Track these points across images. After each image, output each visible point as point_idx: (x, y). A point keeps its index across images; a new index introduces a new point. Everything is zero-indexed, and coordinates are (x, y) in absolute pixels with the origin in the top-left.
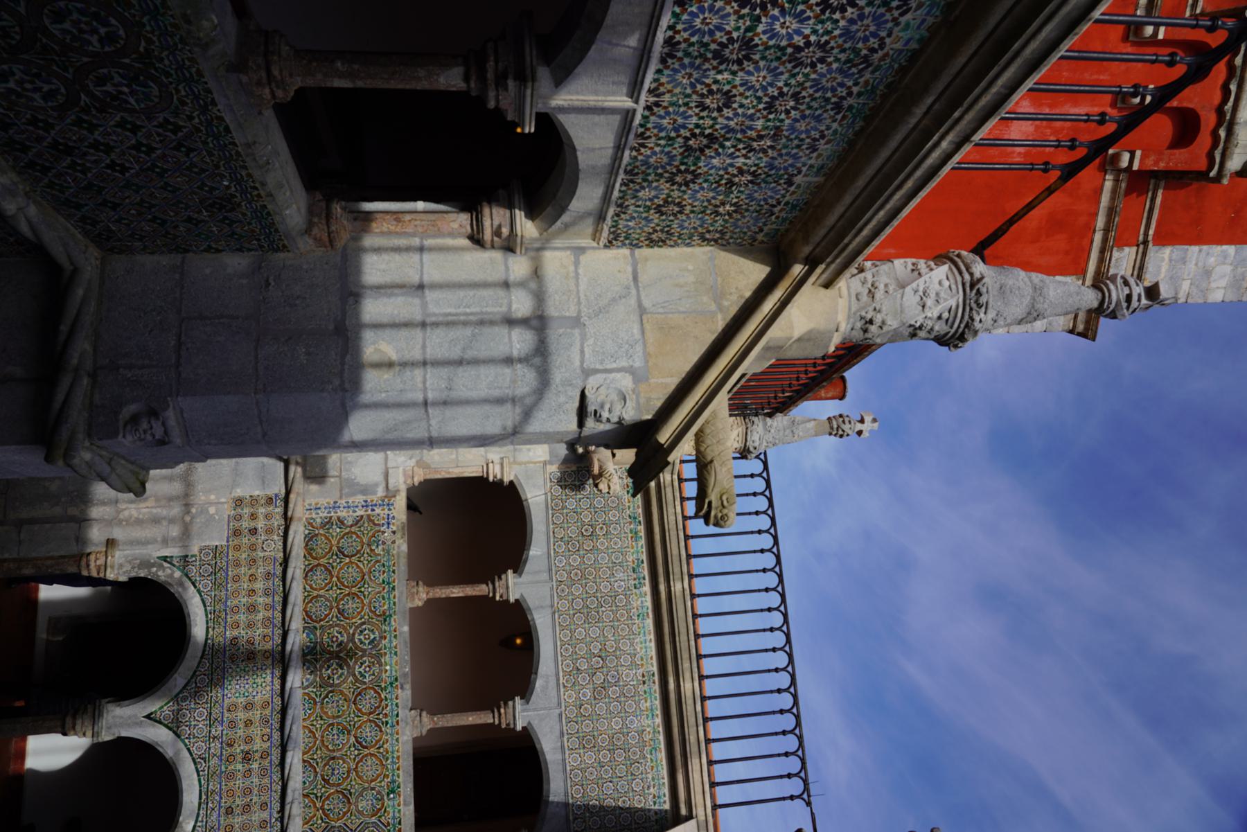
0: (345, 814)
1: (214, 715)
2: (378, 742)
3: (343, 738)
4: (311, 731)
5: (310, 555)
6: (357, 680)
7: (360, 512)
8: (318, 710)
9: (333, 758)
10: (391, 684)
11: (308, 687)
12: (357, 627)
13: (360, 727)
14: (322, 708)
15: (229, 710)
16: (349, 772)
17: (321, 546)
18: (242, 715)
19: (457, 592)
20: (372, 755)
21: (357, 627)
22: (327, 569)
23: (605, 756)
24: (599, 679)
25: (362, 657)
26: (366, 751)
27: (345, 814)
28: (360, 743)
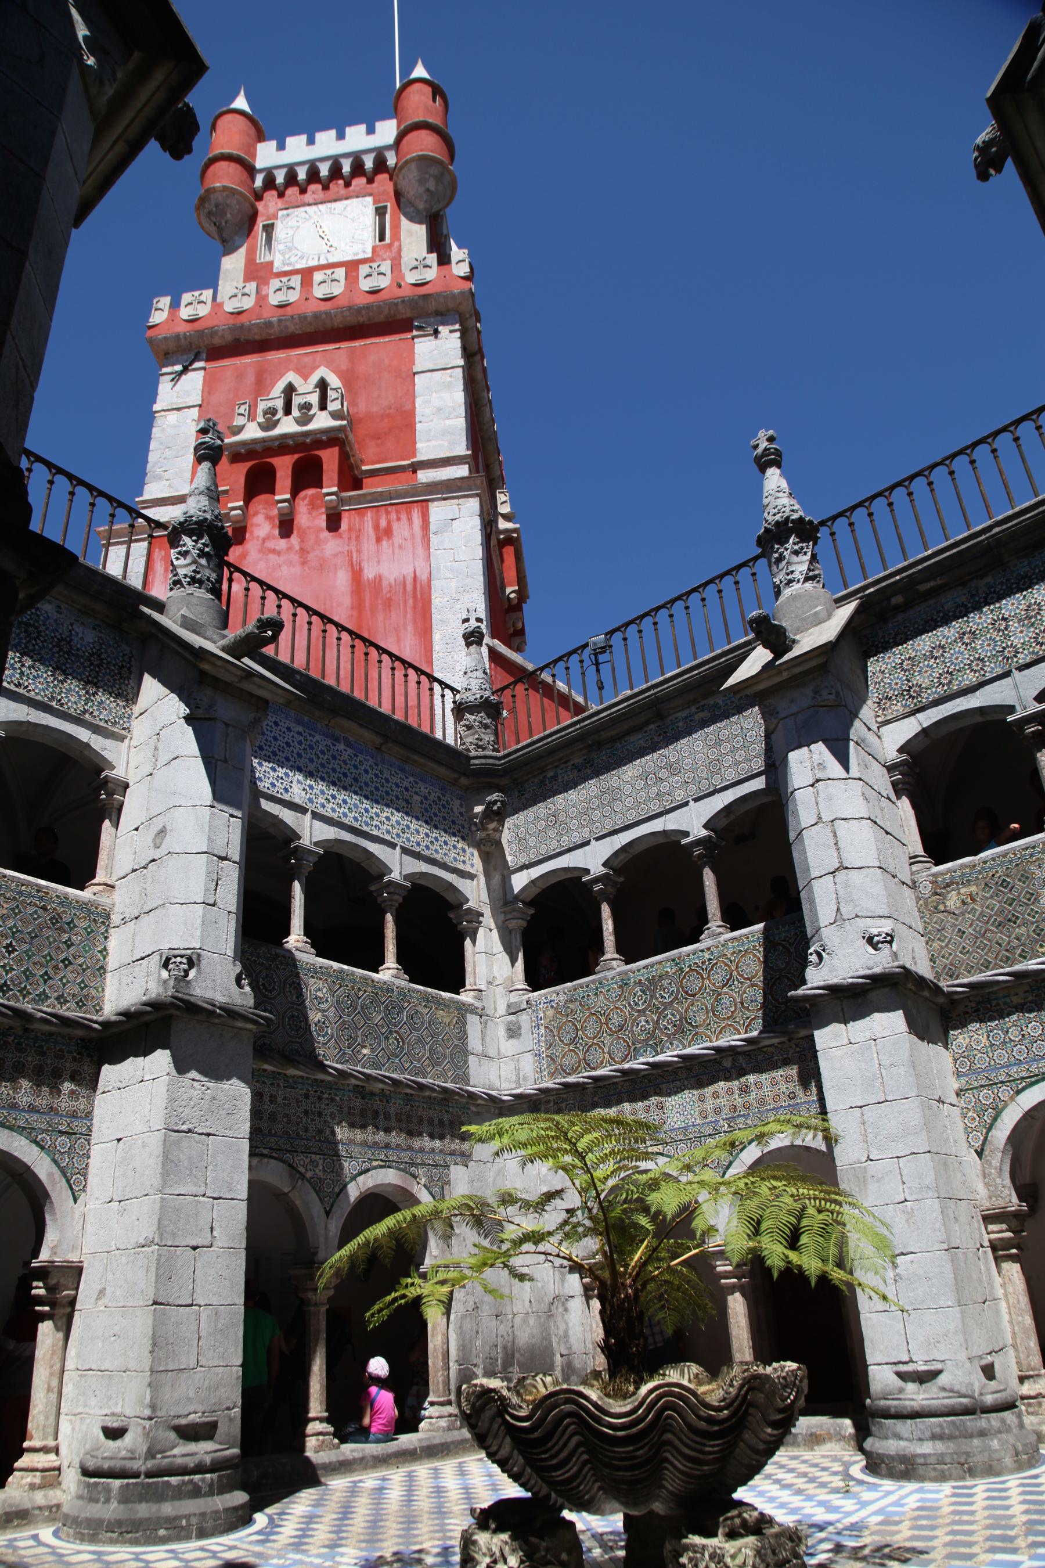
0: (790, 980)
1: (711, 1132)
2: (726, 965)
3: (725, 999)
4: (720, 1032)
5: (577, 1068)
6: (676, 998)
7: (543, 1030)
8: (702, 1030)
9: (742, 1003)
10: (677, 964)
11: (683, 1045)
12: (633, 1009)
13: (714, 985)
14: (700, 1025)
15: (706, 1117)
16: (753, 986)
17: (570, 1060)
18: (710, 1104)
19: (608, 926)
20: (737, 967)
21: (633, 1009)
22: (587, 1051)
23: (725, 748)
24: (663, 773)
25: (656, 999)
26: (735, 973)
27: (790, 980)
28: (728, 981)
